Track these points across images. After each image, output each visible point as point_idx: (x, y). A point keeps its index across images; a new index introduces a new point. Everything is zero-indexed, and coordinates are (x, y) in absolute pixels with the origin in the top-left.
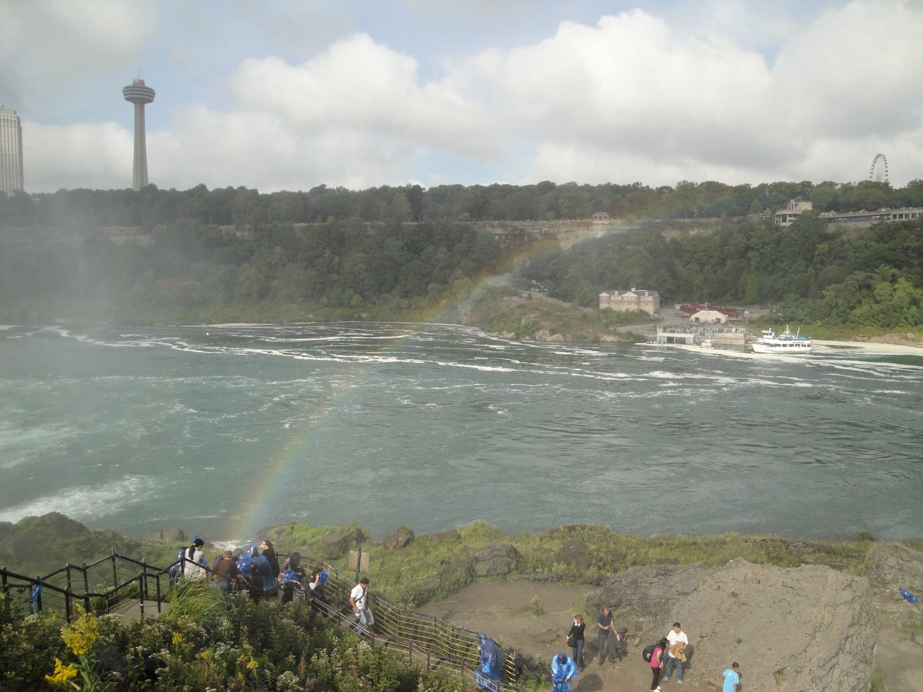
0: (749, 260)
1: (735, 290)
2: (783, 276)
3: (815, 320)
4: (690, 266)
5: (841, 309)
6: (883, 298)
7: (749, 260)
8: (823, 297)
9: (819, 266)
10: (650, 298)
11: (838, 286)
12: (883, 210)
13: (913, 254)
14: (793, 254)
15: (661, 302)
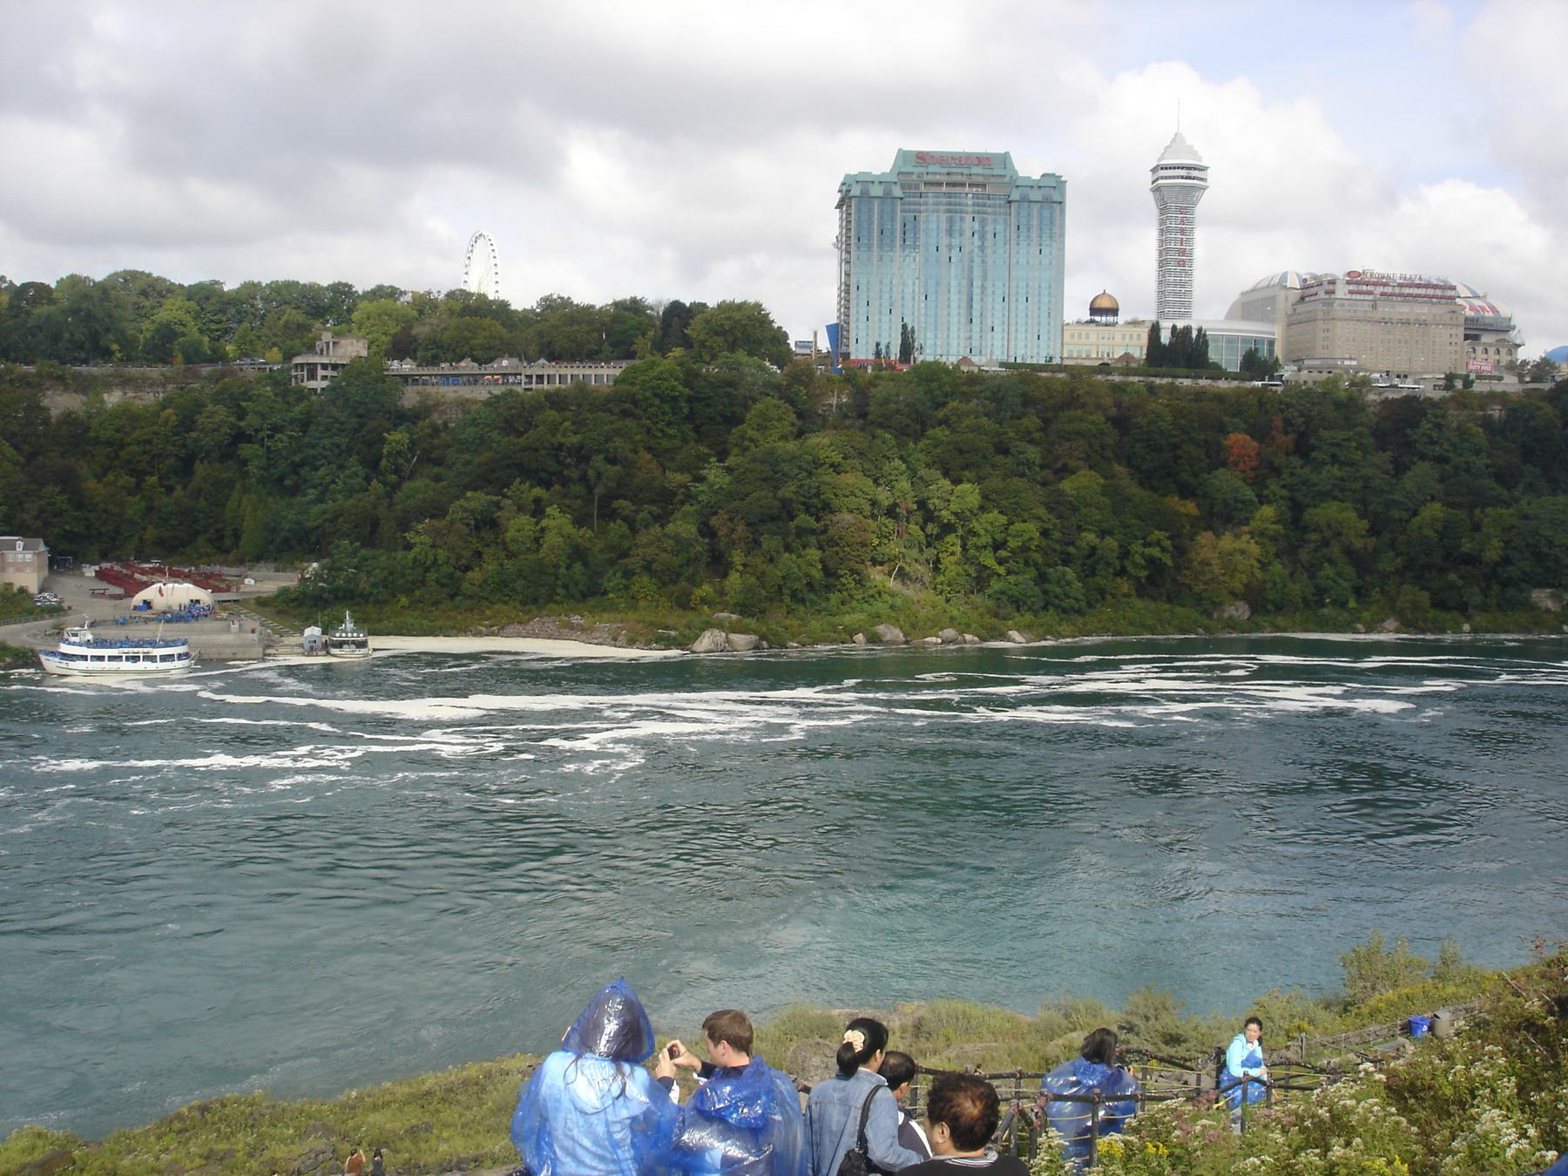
0: (245, 462)
1: (217, 531)
2: (320, 500)
3: (394, 596)
4: (111, 477)
5: (446, 569)
6: (523, 548)
7: (245, 462)
8: (409, 547)
9: (393, 478)
10: (29, 556)
11: (435, 522)
12: (505, 363)
13: (569, 460)
14: (336, 451)
15: (52, 562)
